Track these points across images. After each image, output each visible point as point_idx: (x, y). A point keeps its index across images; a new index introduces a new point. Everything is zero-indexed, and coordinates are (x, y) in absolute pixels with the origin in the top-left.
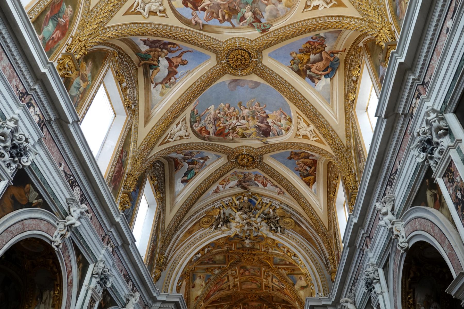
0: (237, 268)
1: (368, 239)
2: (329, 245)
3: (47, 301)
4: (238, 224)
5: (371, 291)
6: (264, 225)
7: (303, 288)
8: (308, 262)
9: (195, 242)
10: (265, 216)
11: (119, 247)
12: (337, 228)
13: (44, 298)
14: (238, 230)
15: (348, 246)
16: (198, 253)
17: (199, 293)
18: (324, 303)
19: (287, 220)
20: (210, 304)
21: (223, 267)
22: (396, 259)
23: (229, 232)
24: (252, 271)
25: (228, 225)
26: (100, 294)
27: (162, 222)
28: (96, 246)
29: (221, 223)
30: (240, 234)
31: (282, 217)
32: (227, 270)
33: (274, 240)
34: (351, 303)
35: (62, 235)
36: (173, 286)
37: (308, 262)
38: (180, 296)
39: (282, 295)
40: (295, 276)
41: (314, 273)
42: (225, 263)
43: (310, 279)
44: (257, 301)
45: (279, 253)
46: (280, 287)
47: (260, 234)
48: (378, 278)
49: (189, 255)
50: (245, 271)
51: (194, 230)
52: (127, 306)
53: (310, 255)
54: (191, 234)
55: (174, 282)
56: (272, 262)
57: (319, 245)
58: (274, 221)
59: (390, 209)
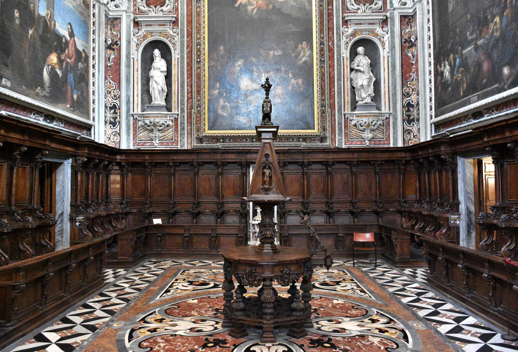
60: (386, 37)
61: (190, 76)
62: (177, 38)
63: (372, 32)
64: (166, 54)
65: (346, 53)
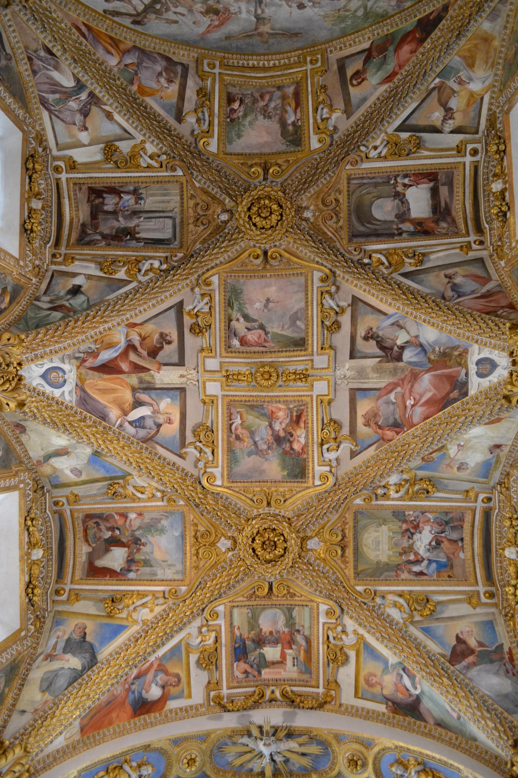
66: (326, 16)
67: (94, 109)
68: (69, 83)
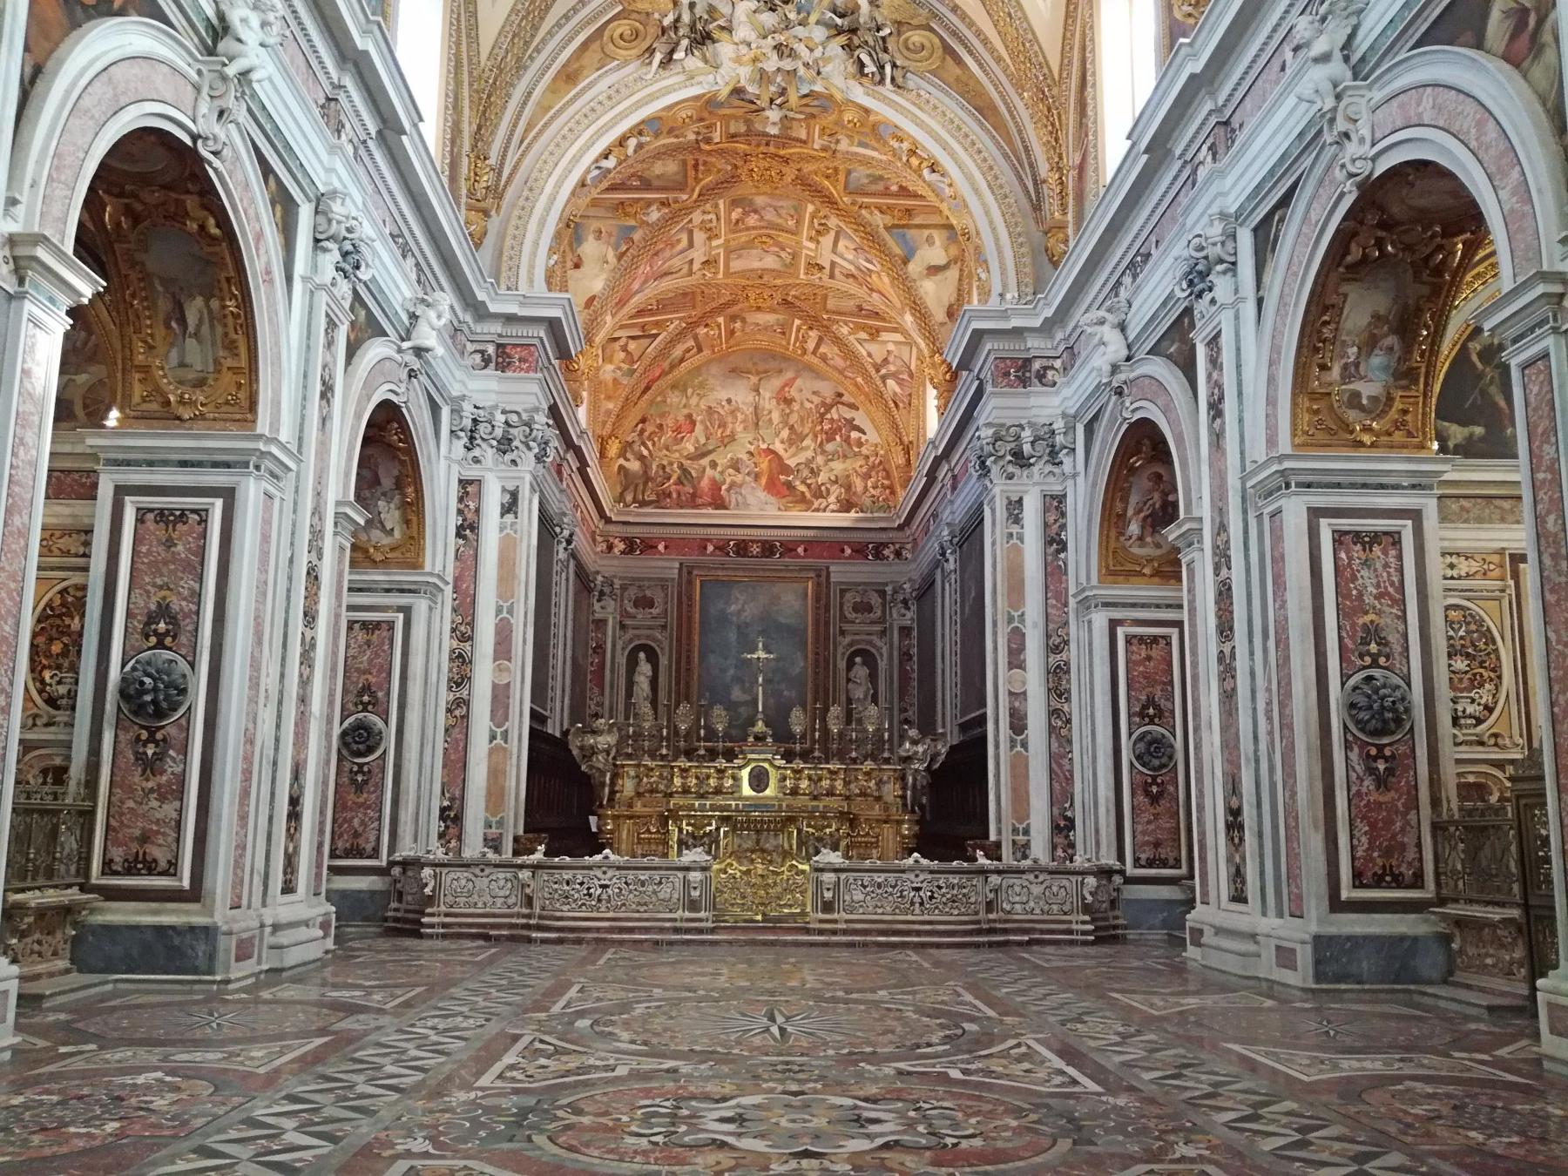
0: (721, 202)
1: (1221, 131)
2: (1054, 133)
3: (205, 329)
4: (743, 49)
5: (1200, 296)
6: (836, 56)
7: (934, 270)
8: (976, 191)
9: (592, 113)
10: (839, 21)
11: (371, 144)
12: (1094, 74)
13: (192, 320)
14: (744, 74)
15: (1145, 152)
16: (606, 155)
17: (597, 285)
18: (1015, 322)
19: (916, 37)
20: (631, 317)
21: (676, 201)
22: (1315, 205)
23: (711, 77)
24: (770, 215)
25: (709, 49)
26: (347, 305)
27: (468, 36)
28: (308, 141)
29: (685, 42)
30: (750, 89)
31: (899, 23)
32: (688, 210)
33: (867, 111)
34: (1114, 327)
35: (221, 114)
36: (532, 267)
37: (976, 191)
38: (566, 303)
39: (861, 292)
40: (913, 232)
41: (994, 230)
42: (681, 187)
43: (977, 248)
44: (773, 311)
45: (875, 154)
46: (858, 268)
47: (818, 88)
48: (1232, 259)
49: (576, 159)
50: (746, 214)
51: (582, 68)
52: (414, 335)
53: (985, 166)
54: (575, 85)
55: (534, 254)
56: (841, 187)
57: (1020, 132)
58: (871, 43)
59: (1341, 38)
60: (885, 650)
61: (678, 683)
62: (666, 644)
63: (870, 643)
64: (653, 658)
65: (842, 664)
66: (712, 389)
67: (879, 361)
68: (891, 383)
